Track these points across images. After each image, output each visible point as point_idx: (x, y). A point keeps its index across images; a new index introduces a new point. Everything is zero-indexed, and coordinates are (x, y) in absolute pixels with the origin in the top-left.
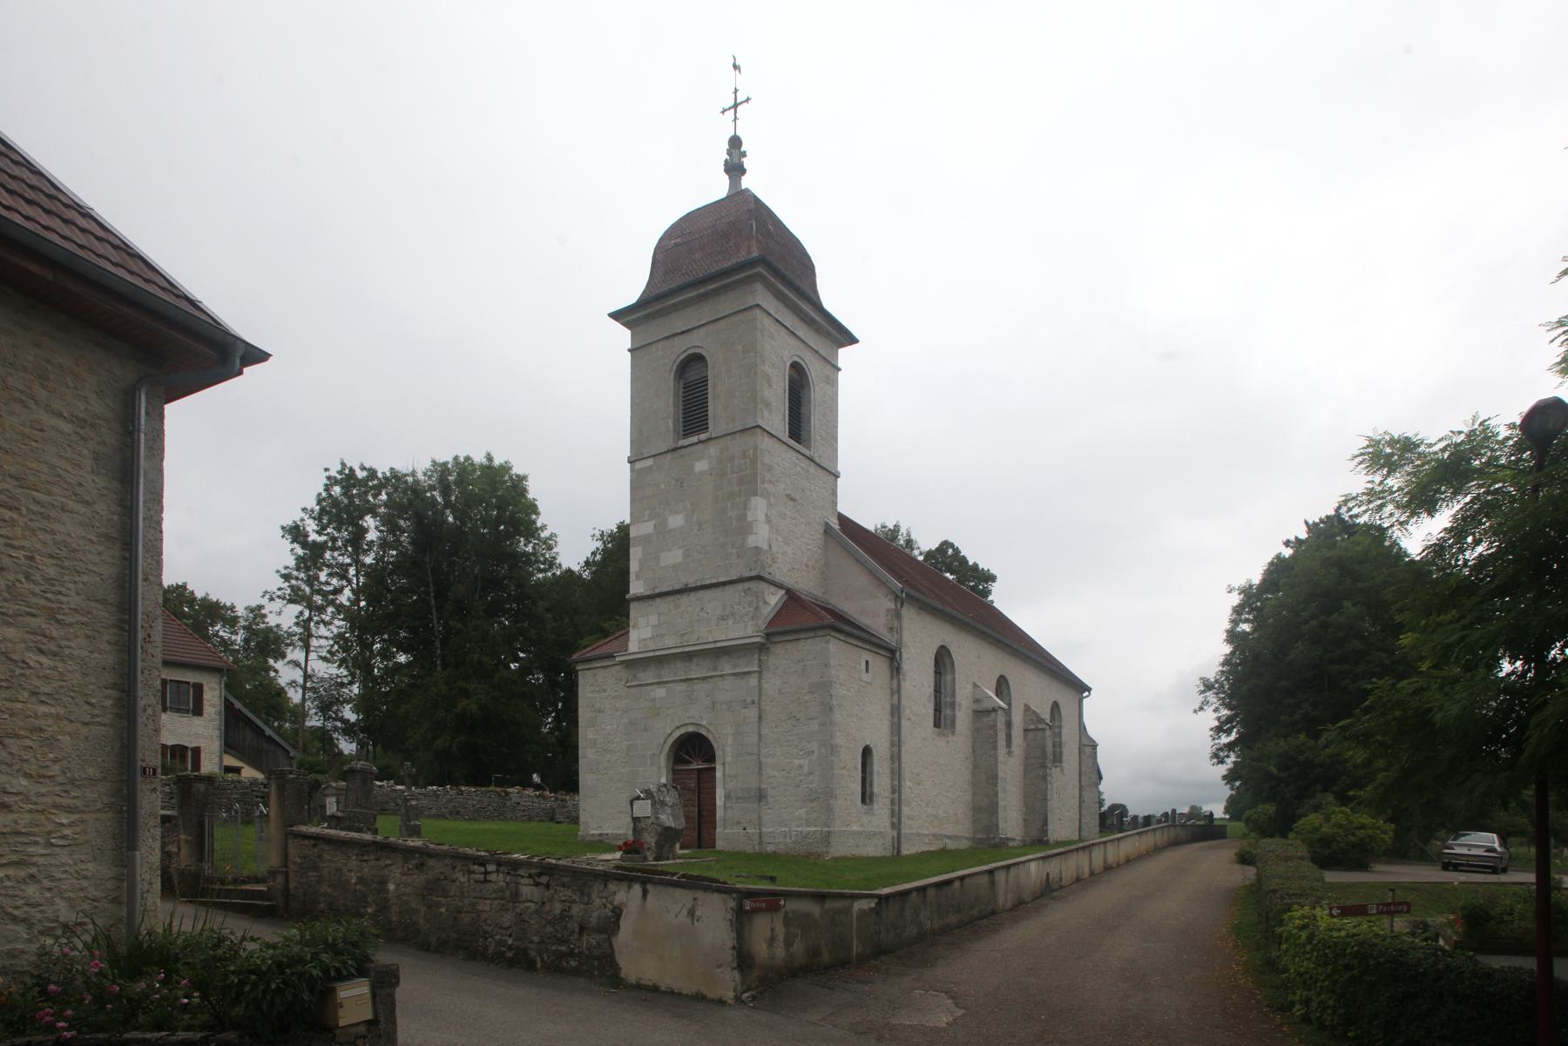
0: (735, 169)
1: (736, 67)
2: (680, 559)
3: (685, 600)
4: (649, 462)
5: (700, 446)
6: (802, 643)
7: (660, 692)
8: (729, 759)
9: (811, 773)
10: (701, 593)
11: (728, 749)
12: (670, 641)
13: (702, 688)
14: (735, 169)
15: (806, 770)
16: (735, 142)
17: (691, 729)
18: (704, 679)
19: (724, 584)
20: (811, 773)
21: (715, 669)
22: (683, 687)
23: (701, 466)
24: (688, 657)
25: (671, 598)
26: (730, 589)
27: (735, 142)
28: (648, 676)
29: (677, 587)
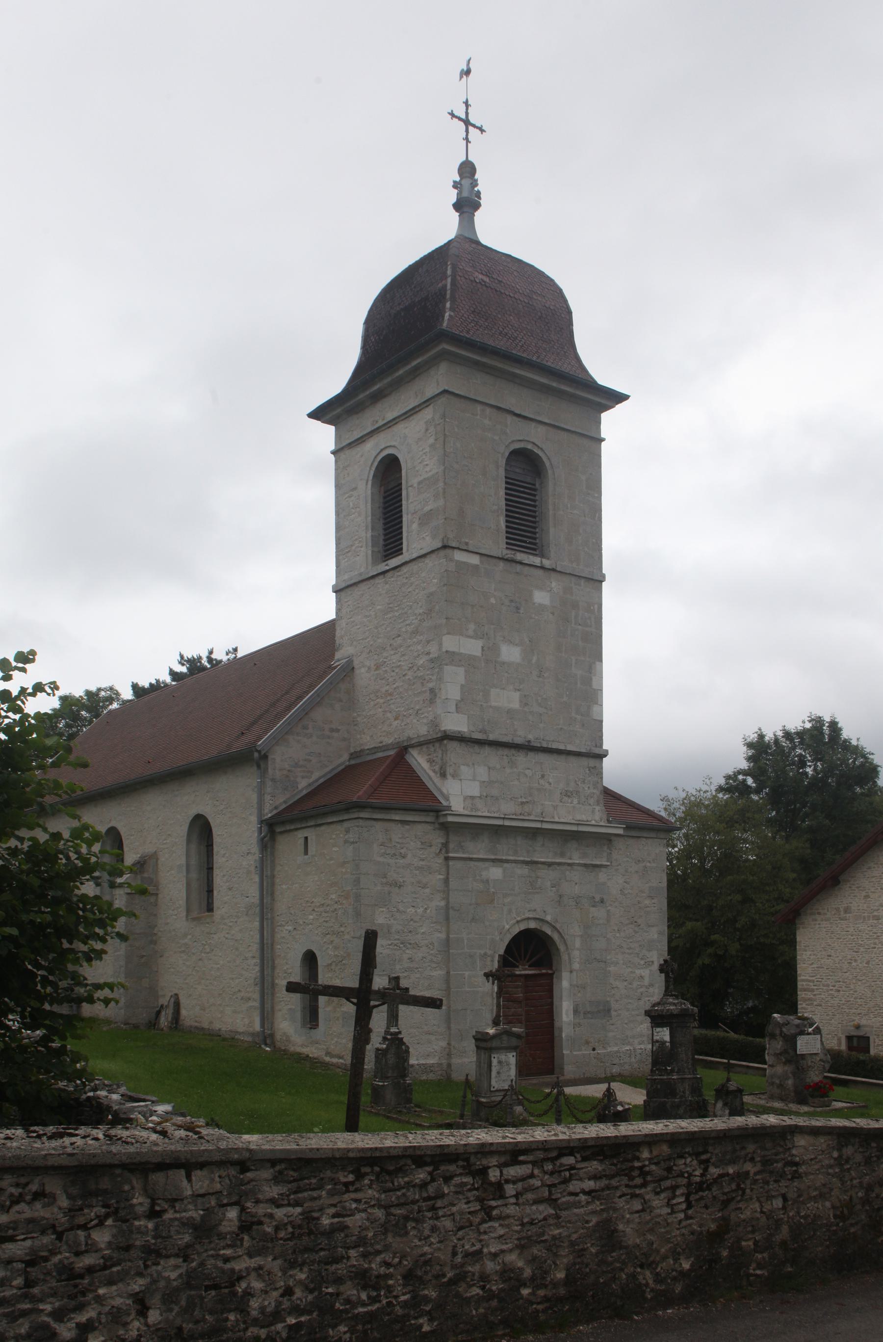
0: (467, 204)
1: (468, 72)
2: (516, 705)
3: (523, 760)
4: (475, 560)
5: (540, 572)
6: (643, 841)
7: (495, 873)
8: (576, 966)
9: (651, 985)
10: (542, 757)
11: (576, 953)
12: (507, 808)
13: (547, 876)
14: (467, 204)
15: (646, 982)
16: (467, 170)
17: (532, 925)
18: (550, 864)
19: (559, 752)
20: (651, 985)
21: (562, 855)
22: (524, 870)
23: (541, 597)
24: (533, 834)
25: (506, 751)
26: (574, 761)
27: (467, 170)
28: (479, 848)
29: (518, 740)
